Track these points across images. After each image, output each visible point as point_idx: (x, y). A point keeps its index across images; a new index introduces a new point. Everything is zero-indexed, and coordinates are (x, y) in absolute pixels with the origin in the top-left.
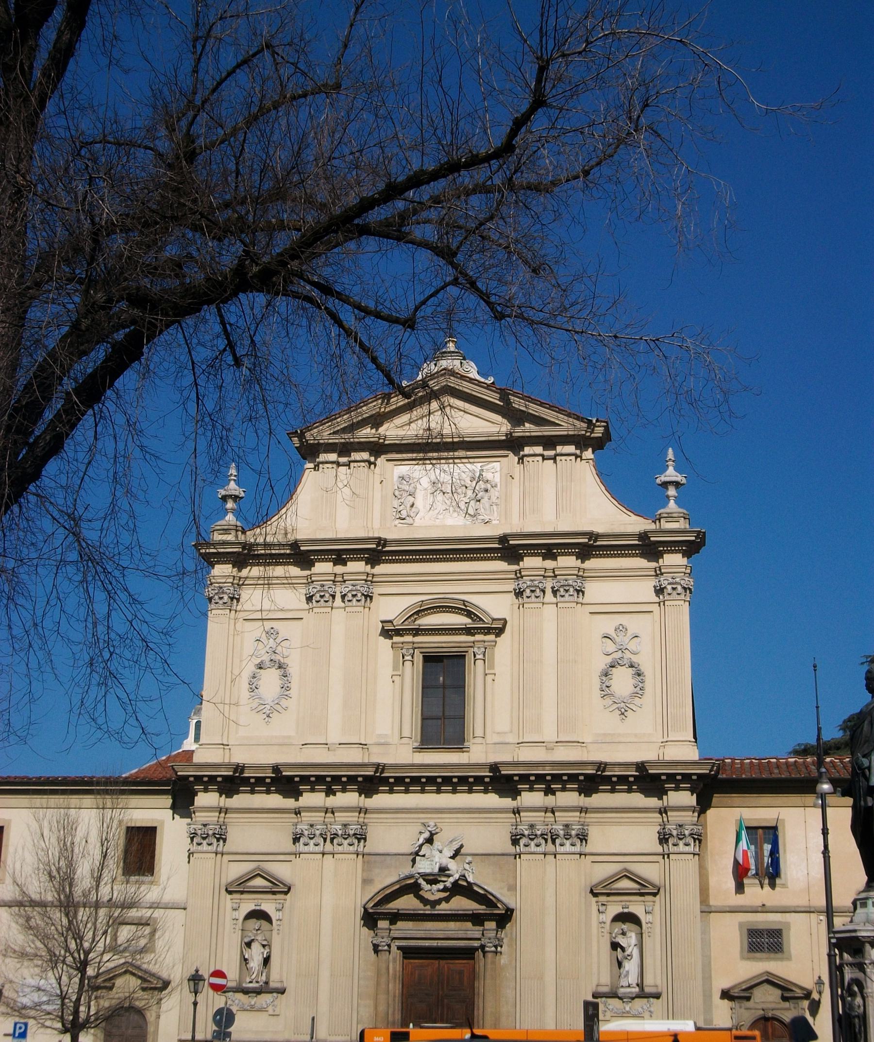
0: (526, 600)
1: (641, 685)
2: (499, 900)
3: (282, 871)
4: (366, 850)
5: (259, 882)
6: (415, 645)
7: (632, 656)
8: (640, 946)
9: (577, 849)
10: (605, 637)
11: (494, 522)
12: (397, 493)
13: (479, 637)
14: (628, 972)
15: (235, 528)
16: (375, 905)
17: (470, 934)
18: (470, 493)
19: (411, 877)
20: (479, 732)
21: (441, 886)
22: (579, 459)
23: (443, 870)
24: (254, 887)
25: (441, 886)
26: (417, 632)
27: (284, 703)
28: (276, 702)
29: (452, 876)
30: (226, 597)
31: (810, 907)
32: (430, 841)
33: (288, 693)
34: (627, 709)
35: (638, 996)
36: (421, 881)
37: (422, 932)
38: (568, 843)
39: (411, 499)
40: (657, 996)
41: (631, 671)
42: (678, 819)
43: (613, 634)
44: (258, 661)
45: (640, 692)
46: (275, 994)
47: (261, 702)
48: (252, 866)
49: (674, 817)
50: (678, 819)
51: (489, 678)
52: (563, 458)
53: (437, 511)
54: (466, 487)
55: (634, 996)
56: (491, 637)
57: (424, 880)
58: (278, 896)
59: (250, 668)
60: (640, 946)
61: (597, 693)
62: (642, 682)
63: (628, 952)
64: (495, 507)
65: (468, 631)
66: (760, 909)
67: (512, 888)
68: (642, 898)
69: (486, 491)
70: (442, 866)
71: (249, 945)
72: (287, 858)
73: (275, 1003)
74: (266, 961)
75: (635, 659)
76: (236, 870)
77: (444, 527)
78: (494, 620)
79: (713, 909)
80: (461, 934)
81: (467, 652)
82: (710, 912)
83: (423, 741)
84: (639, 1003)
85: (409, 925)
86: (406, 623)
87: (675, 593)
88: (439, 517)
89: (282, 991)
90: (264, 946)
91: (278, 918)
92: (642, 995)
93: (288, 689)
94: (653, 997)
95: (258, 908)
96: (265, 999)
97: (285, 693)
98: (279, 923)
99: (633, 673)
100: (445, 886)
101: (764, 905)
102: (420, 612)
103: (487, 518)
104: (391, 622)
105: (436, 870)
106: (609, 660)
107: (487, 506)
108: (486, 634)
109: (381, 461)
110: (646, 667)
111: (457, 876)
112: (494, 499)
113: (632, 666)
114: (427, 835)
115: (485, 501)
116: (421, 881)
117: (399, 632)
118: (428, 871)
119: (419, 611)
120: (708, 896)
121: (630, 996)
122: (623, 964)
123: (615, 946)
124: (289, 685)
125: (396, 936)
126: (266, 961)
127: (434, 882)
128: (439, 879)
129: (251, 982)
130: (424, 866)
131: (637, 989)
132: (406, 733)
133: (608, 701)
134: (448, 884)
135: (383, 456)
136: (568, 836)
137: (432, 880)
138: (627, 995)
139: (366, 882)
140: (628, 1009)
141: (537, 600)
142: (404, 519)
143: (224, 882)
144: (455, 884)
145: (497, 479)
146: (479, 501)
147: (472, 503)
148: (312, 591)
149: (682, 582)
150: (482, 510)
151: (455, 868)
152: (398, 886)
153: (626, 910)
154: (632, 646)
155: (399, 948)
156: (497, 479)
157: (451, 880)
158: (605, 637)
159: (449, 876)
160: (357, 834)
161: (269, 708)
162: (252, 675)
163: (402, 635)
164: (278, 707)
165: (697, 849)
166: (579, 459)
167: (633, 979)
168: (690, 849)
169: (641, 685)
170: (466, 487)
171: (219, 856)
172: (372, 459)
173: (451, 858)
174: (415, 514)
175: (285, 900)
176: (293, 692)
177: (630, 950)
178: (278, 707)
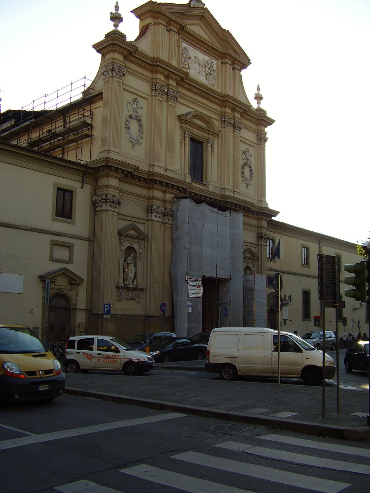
0: (226, 126)
3: (141, 227)
11: (215, 87)
20: (209, 179)
24: (130, 235)
26: (193, 125)
28: (137, 139)
31: (281, 270)
44: (130, 114)
58: (140, 241)
61: (240, 174)
62: (252, 174)
66: (270, 269)
72: (144, 222)
73: (139, 296)
77: (200, 80)
89: (142, 290)
91: (140, 252)
93: (142, 133)
95: (131, 246)
98: (140, 255)
101: (271, 268)
106: (243, 162)
115: (212, 75)
117: (186, 122)
119: (194, 115)
124: (143, 131)
142: (187, 69)
146: (211, 75)
154: (249, 158)
163: (186, 124)
170: (206, 66)
176: (144, 136)
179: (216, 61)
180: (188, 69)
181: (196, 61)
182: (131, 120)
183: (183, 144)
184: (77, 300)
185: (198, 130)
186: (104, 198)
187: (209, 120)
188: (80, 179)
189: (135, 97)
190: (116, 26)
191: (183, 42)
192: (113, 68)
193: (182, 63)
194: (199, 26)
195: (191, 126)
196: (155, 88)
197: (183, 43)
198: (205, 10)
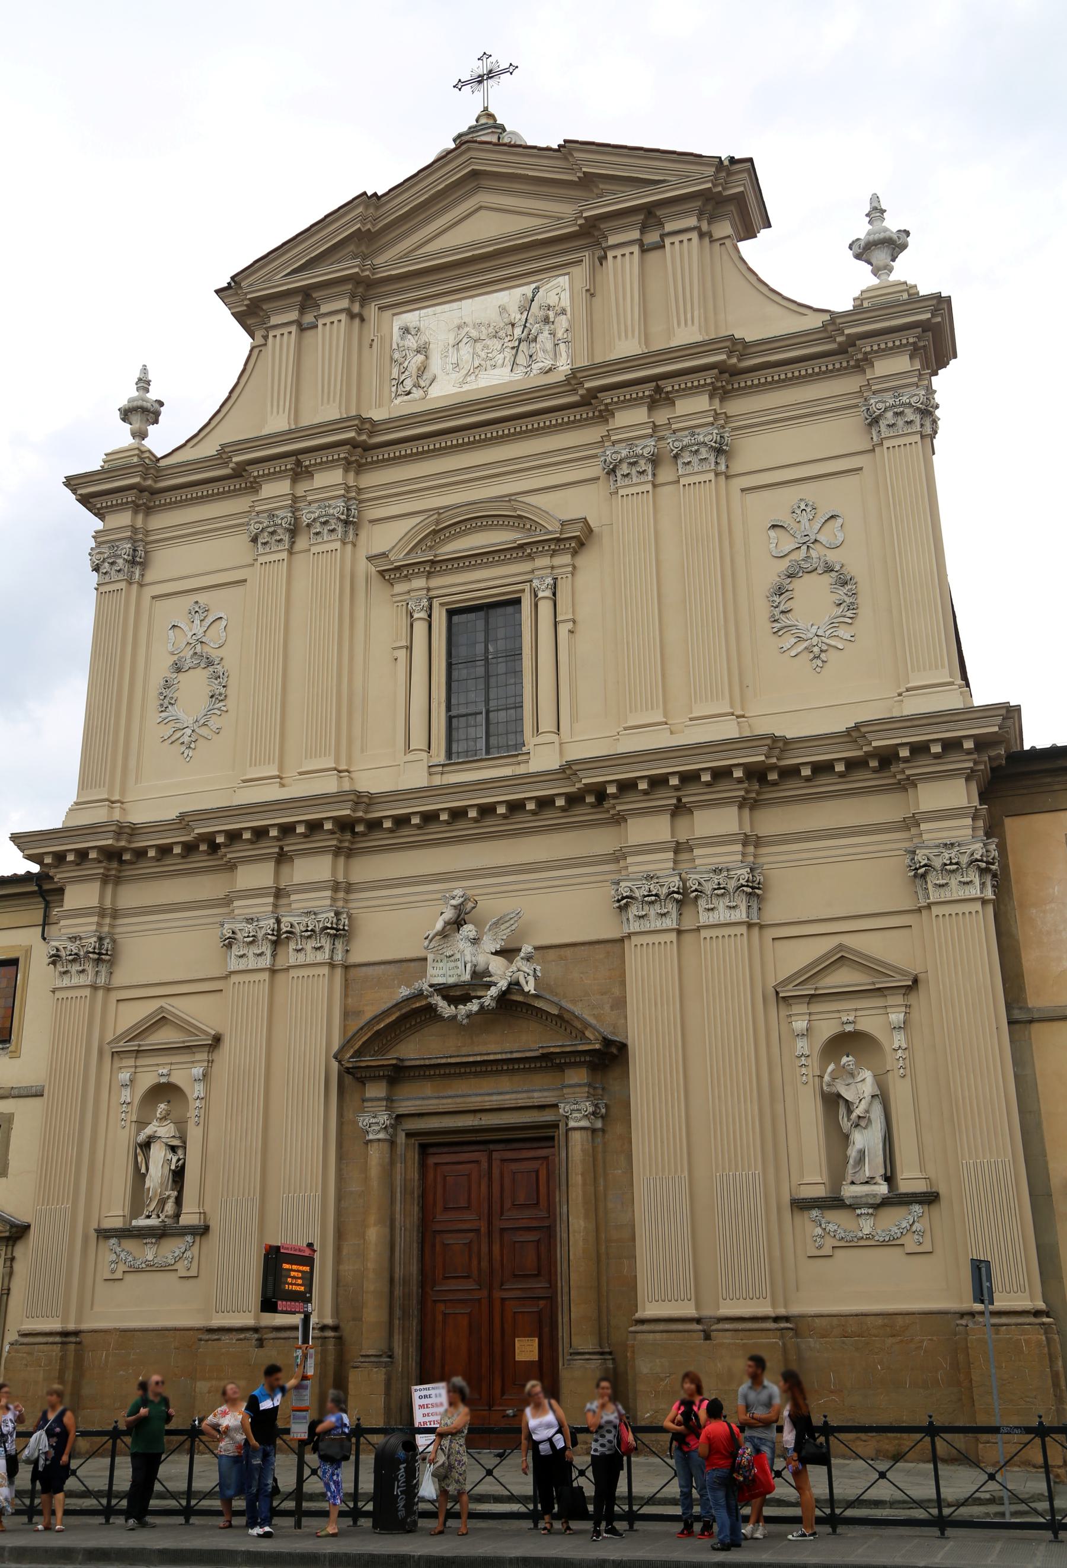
1: (848, 600)
2: (587, 1025)
4: (355, 958)
5: (165, 1036)
6: (433, 593)
7: (823, 551)
8: (882, 1097)
9: (740, 915)
10: (774, 526)
12: (396, 356)
13: (543, 561)
14: (862, 1153)
15: (136, 452)
16: (358, 1053)
17: (539, 1097)
18: (518, 331)
19: (420, 995)
20: (547, 722)
21: (474, 1006)
22: (707, 240)
23: (480, 978)
25: (474, 1006)
26: (434, 567)
27: (214, 722)
28: (202, 722)
29: (495, 984)
30: (120, 561)
32: (458, 923)
33: (221, 704)
34: (824, 648)
35: (885, 1203)
36: (438, 1001)
37: (449, 1101)
38: (721, 904)
39: (420, 358)
40: (930, 1199)
41: (828, 579)
42: (945, 834)
43: (787, 520)
45: (849, 614)
46: (189, 1238)
47: (177, 725)
48: (154, 1005)
49: (932, 832)
50: (945, 834)
51: (563, 629)
52: (676, 239)
53: (464, 372)
54: (513, 325)
55: (878, 1201)
56: (565, 559)
57: (444, 998)
59: (161, 667)
60: (882, 1097)
61: (764, 625)
63: (858, 1111)
64: (562, 346)
65: (521, 551)
67: (620, 1004)
68: (879, 1002)
69: (546, 320)
70: (480, 968)
71: (146, 1146)
74: (178, 1175)
75: (832, 557)
76: (133, 1015)
78: (563, 524)
79: (1036, 1016)
80: (522, 1100)
81: (523, 591)
82: (1031, 1022)
83: (449, 754)
84: (894, 1220)
85: (427, 1089)
86: (413, 555)
87: (900, 422)
88: (469, 379)
90: (173, 1149)
92: (896, 1200)
94: (920, 1203)
96: (172, 1248)
97: (217, 706)
99: (833, 581)
100: (482, 1007)
102: (439, 533)
103: (548, 363)
104: (384, 555)
105: (467, 977)
106: (785, 564)
107: (549, 346)
108: (554, 553)
109: (372, 311)
110: (855, 568)
111: (503, 984)
112: (560, 334)
113: (829, 569)
114: (449, 914)
115: (544, 337)
116: (438, 1001)
118: (451, 981)
119: (435, 532)
120: (1021, 988)
121: (871, 1201)
122: (851, 1138)
123: (833, 1101)
125: (401, 1111)
126: (178, 1175)
127: (466, 999)
128: (473, 994)
129: (149, 1217)
130: (441, 973)
131: (883, 1189)
132: (418, 740)
133: (789, 640)
134: (487, 1001)
135: (373, 304)
136: (721, 891)
137: (456, 994)
138: (864, 1200)
139: (346, 1014)
140: (867, 1230)
141: (643, 478)
142: (409, 393)
143: (110, 1037)
144: (503, 998)
145: (566, 302)
146: (535, 340)
147: (523, 346)
148: (253, 529)
149: (913, 400)
150: (541, 354)
151: (501, 973)
152: (397, 1014)
153: (849, 1028)
155: (409, 1135)
156: (566, 302)
157: (493, 991)
158: (774, 526)
159: (489, 986)
160: (327, 928)
161: (188, 731)
162: (162, 682)
164: (204, 731)
165: (989, 894)
166: (707, 240)
167: (874, 1166)
168: (974, 891)
169: (848, 600)
171: (100, 993)
172: (356, 308)
173: (496, 953)
174: (428, 383)
175: (211, 1062)
177: (863, 1106)
178: (204, 731)
179: (568, 274)
180: (414, 390)
181: (458, 340)
182: (182, 676)
183: (402, 654)
184: (9, 1290)
185: (459, 570)
186: (94, 948)
187: (515, 510)
188: (38, 916)
189: (188, 601)
190: (140, 435)
191: (394, 315)
192: (134, 557)
193: (394, 382)
194: (482, 212)
195: (429, 575)
196: (348, 516)
197: (395, 318)
198: (469, 149)
